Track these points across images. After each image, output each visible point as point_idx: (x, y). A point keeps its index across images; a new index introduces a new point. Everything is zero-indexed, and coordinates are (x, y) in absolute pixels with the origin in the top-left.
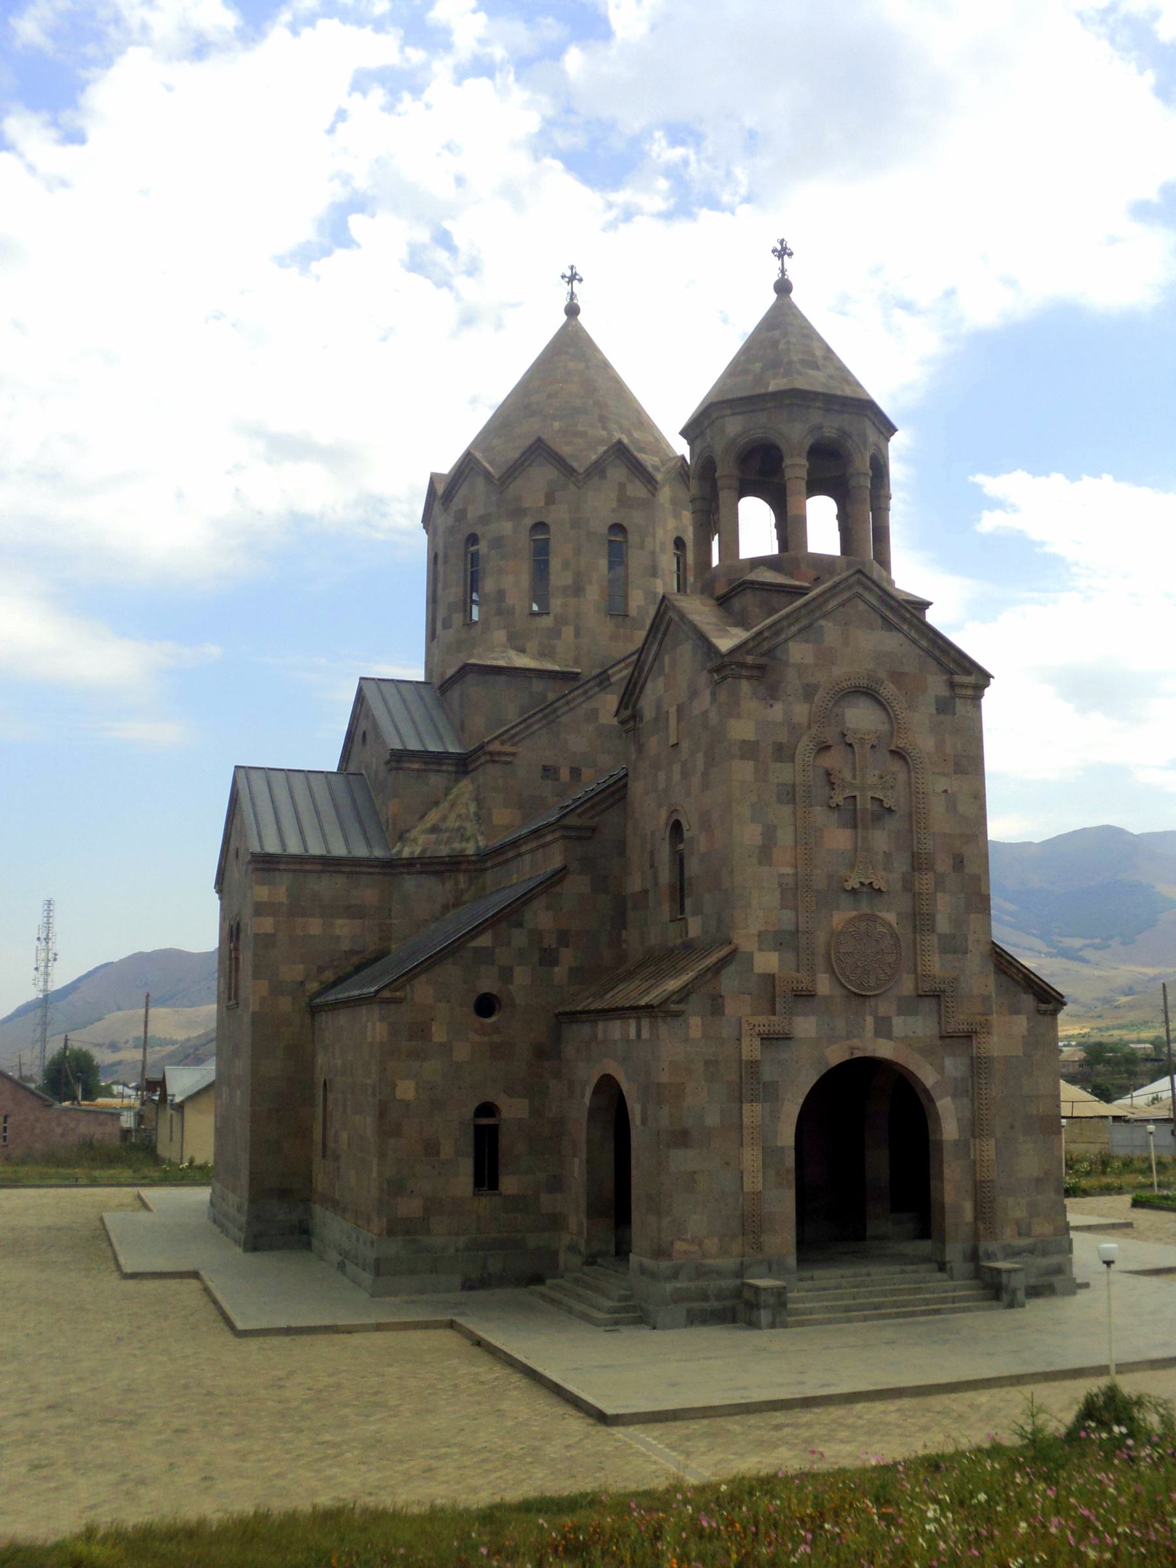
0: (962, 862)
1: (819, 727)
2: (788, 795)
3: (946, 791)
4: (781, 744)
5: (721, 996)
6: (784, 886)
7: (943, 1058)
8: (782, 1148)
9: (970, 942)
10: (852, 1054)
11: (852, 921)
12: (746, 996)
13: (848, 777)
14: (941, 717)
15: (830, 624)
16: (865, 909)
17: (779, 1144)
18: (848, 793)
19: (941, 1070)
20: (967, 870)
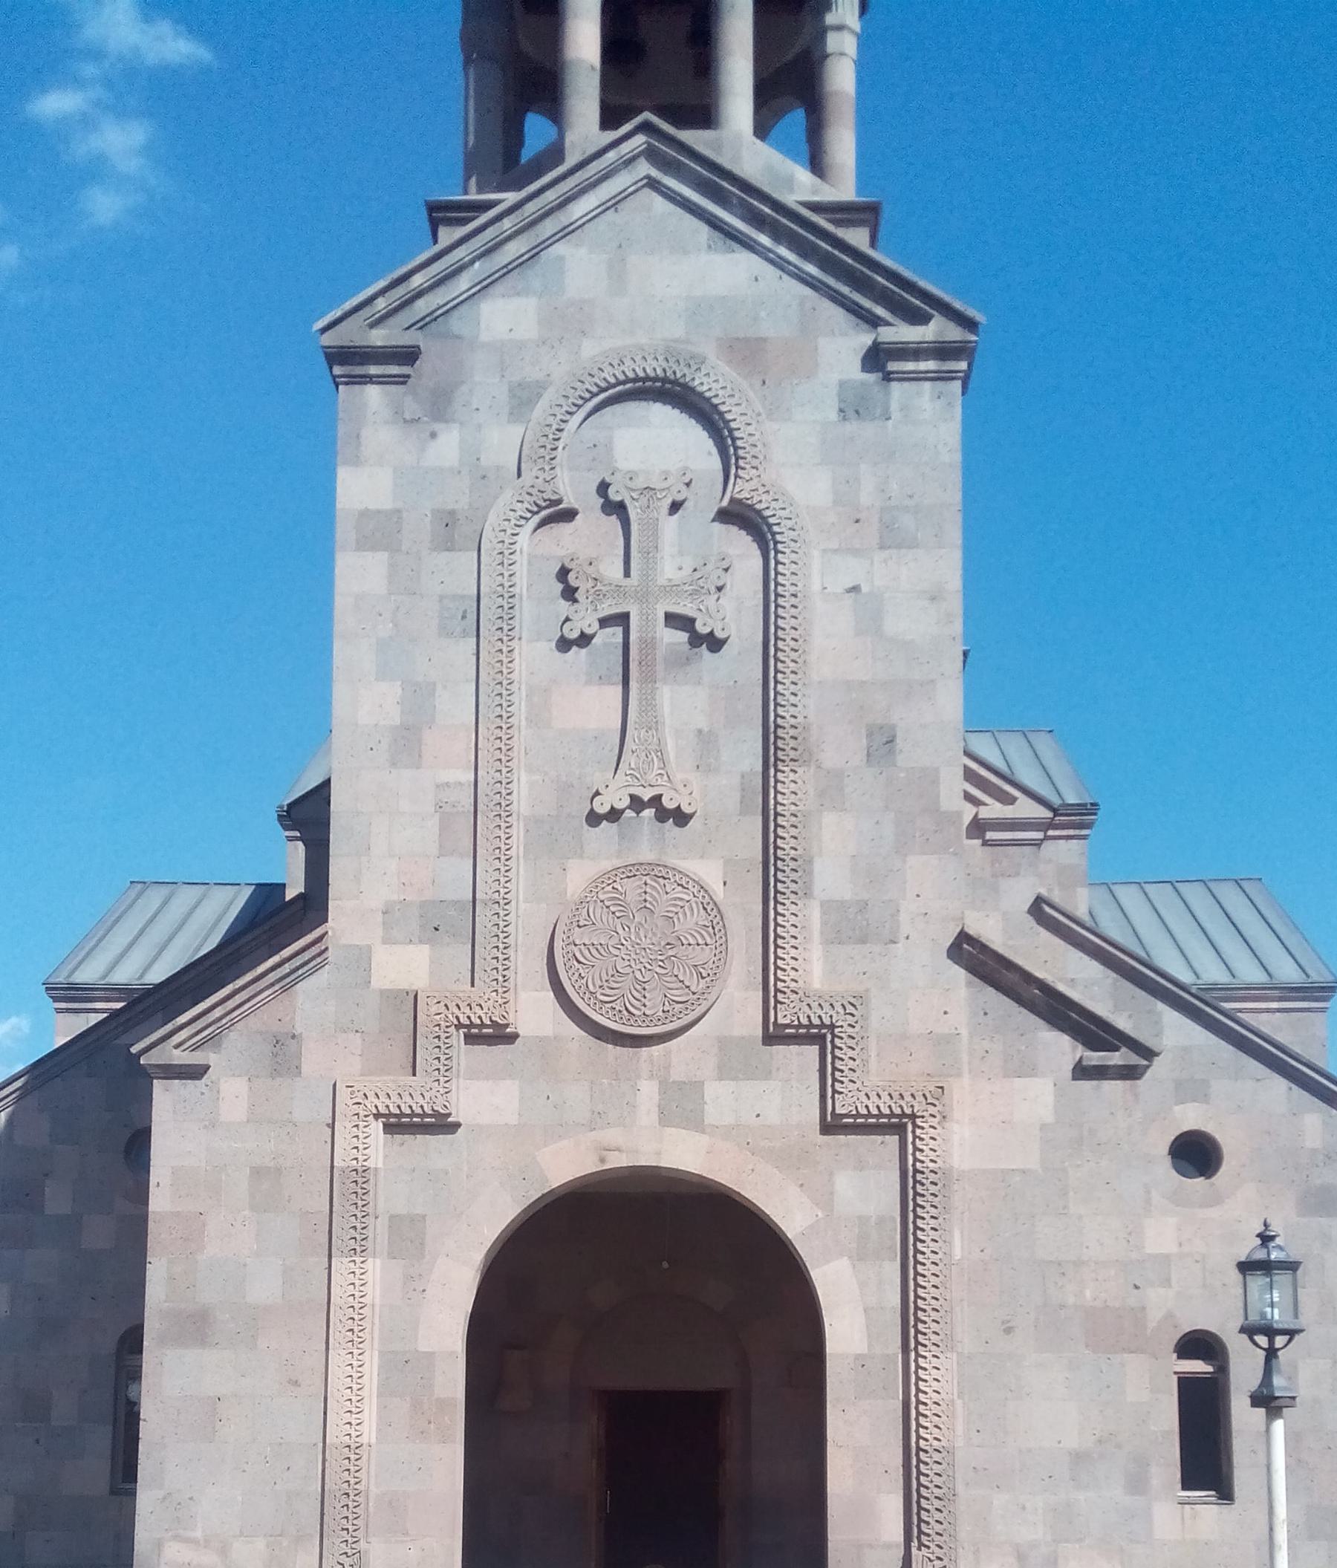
0: (891, 741)
1: (542, 469)
2: (464, 617)
3: (855, 589)
4: (452, 513)
5: (294, 1037)
6: (447, 809)
7: (831, 1174)
8: (431, 1355)
9: (903, 917)
10: (602, 1161)
11: (608, 878)
12: (351, 1035)
13: (612, 569)
14: (852, 427)
15: (583, 251)
16: (646, 853)
17: (423, 1347)
18: (607, 609)
19: (825, 1199)
20: (901, 760)
